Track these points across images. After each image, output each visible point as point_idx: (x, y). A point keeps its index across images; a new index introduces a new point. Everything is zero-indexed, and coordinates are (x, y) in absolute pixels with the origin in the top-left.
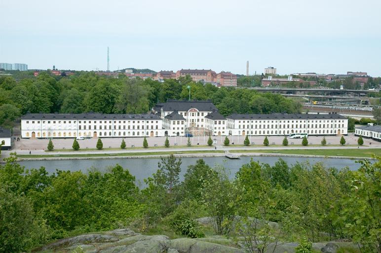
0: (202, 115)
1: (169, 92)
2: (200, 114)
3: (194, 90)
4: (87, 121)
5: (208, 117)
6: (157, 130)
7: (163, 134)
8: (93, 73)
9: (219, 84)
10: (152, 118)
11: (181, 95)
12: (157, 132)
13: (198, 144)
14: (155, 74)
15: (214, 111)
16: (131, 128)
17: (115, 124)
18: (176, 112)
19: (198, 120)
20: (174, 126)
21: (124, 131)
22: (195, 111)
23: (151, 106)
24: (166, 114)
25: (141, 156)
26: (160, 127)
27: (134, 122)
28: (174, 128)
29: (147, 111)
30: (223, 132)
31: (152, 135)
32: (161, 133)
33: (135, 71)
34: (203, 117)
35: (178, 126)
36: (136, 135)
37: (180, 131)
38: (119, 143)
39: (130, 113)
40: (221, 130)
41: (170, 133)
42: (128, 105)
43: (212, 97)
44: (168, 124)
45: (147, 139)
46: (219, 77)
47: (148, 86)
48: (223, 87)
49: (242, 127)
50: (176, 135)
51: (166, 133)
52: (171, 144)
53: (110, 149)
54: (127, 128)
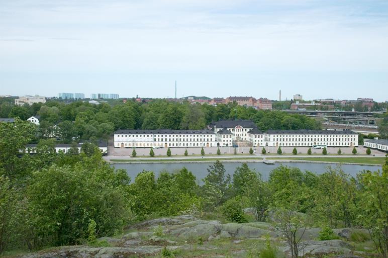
0: (246, 131)
1: (221, 113)
2: (244, 130)
3: (239, 112)
4: (160, 135)
6: (211, 142)
7: (216, 145)
8: (165, 100)
9: (258, 107)
10: (207, 133)
11: (229, 116)
12: (211, 144)
14: (210, 100)
15: (254, 128)
16: (192, 140)
17: (180, 138)
18: (225, 128)
19: (242, 135)
20: (224, 139)
21: (198, 142)
22: (240, 128)
23: (207, 124)
24: (218, 130)
25: (200, 162)
27: (194, 136)
28: (224, 141)
29: (204, 128)
30: (261, 144)
31: (208, 146)
32: (215, 144)
33: (195, 98)
34: (246, 133)
35: (227, 139)
36: (196, 146)
37: (229, 143)
38: (183, 151)
39: (191, 130)
40: (260, 142)
41: (221, 144)
42: (191, 123)
43: (253, 117)
44: (219, 138)
45: (204, 148)
46: (258, 102)
47: (205, 109)
48: (262, 110)
49: (276, 140)
51: (218, 144)
52: (222, 152)
53: (176, 156)
54: (189, 140)
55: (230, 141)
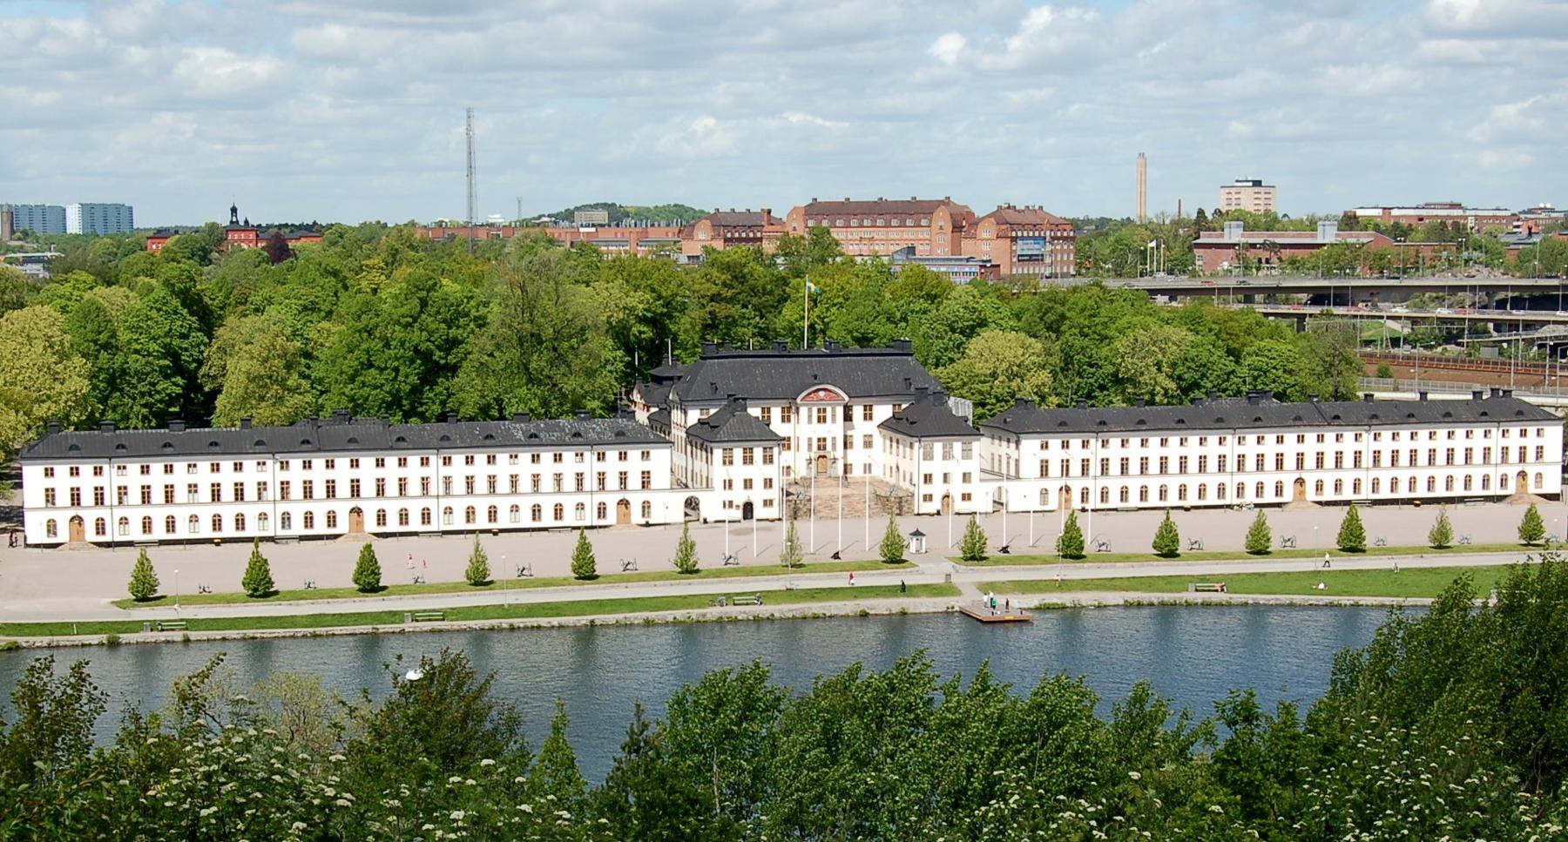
0: (868, 417)
5: (900, 426)
6: (646, 496)
7: (676, 513)
12: (646, 507)
13: (836, 556)
18: (737, 402)
24: (694, 416)
26: (661, 479)
28: (729, 484)
30: (966, 497)
31: (624, 517)
32: (669, 507)
34: (871, 428)
36: (547, 519)
37: (757, 495)
41: (711, 507)
44: (699, 465)
49: (1055, 469)
50: (739, 514)
51: (691, 504)
52: (705, 558)
55: (768, 483)
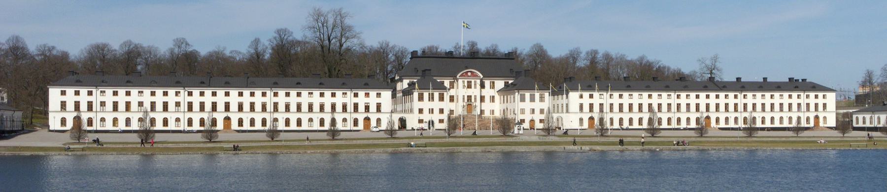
2: (487, 83)
19: (482, 99)
22: (474, 75)
28: (421, 111)
35: (431, 105)
